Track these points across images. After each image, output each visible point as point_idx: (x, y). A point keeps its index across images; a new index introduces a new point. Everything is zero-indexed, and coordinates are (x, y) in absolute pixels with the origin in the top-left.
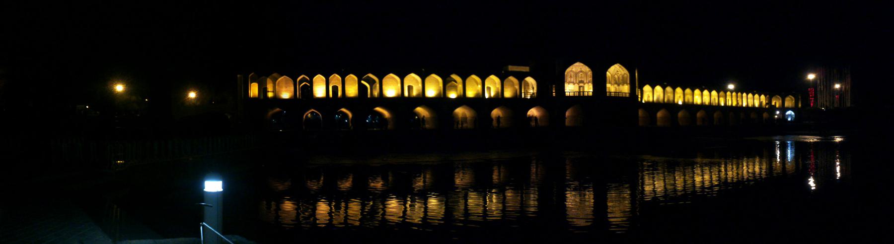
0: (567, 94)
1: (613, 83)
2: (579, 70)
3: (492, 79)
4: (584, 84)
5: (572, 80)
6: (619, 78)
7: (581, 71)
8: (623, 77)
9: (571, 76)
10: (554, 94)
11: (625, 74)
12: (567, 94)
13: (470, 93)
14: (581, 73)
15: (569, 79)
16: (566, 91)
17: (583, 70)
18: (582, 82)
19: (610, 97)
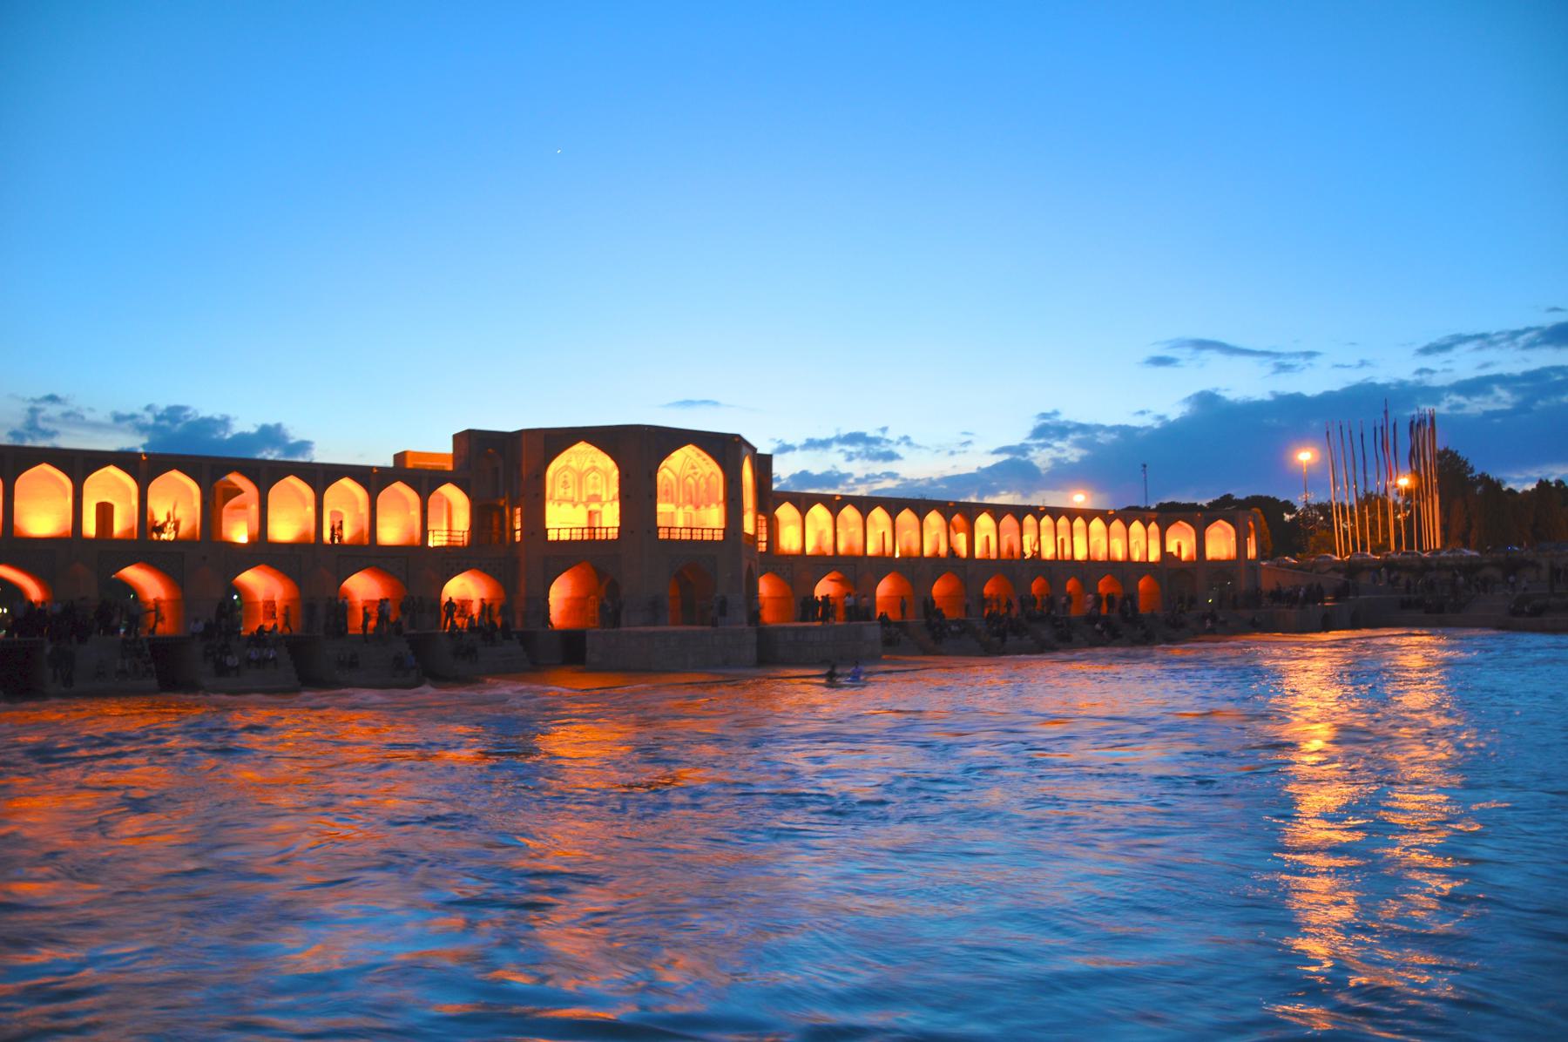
0: (552, 536)
1: (681, 501)
2: (588, 465)
3: (396, 491)
4: (602, 506)
5: (570, 493)
6: (697, 484)
7: (594, 469)
8: (707, 482)
9: (565, 482)
10: (518, 534)
11: (712, 473)
12: (552, 536)
13: (390, 533)
14: (594, 474)
15: (561, 491)
16: (548, 526)
17: (598, 464)
18: (596, 498)
19: (670, 542)
